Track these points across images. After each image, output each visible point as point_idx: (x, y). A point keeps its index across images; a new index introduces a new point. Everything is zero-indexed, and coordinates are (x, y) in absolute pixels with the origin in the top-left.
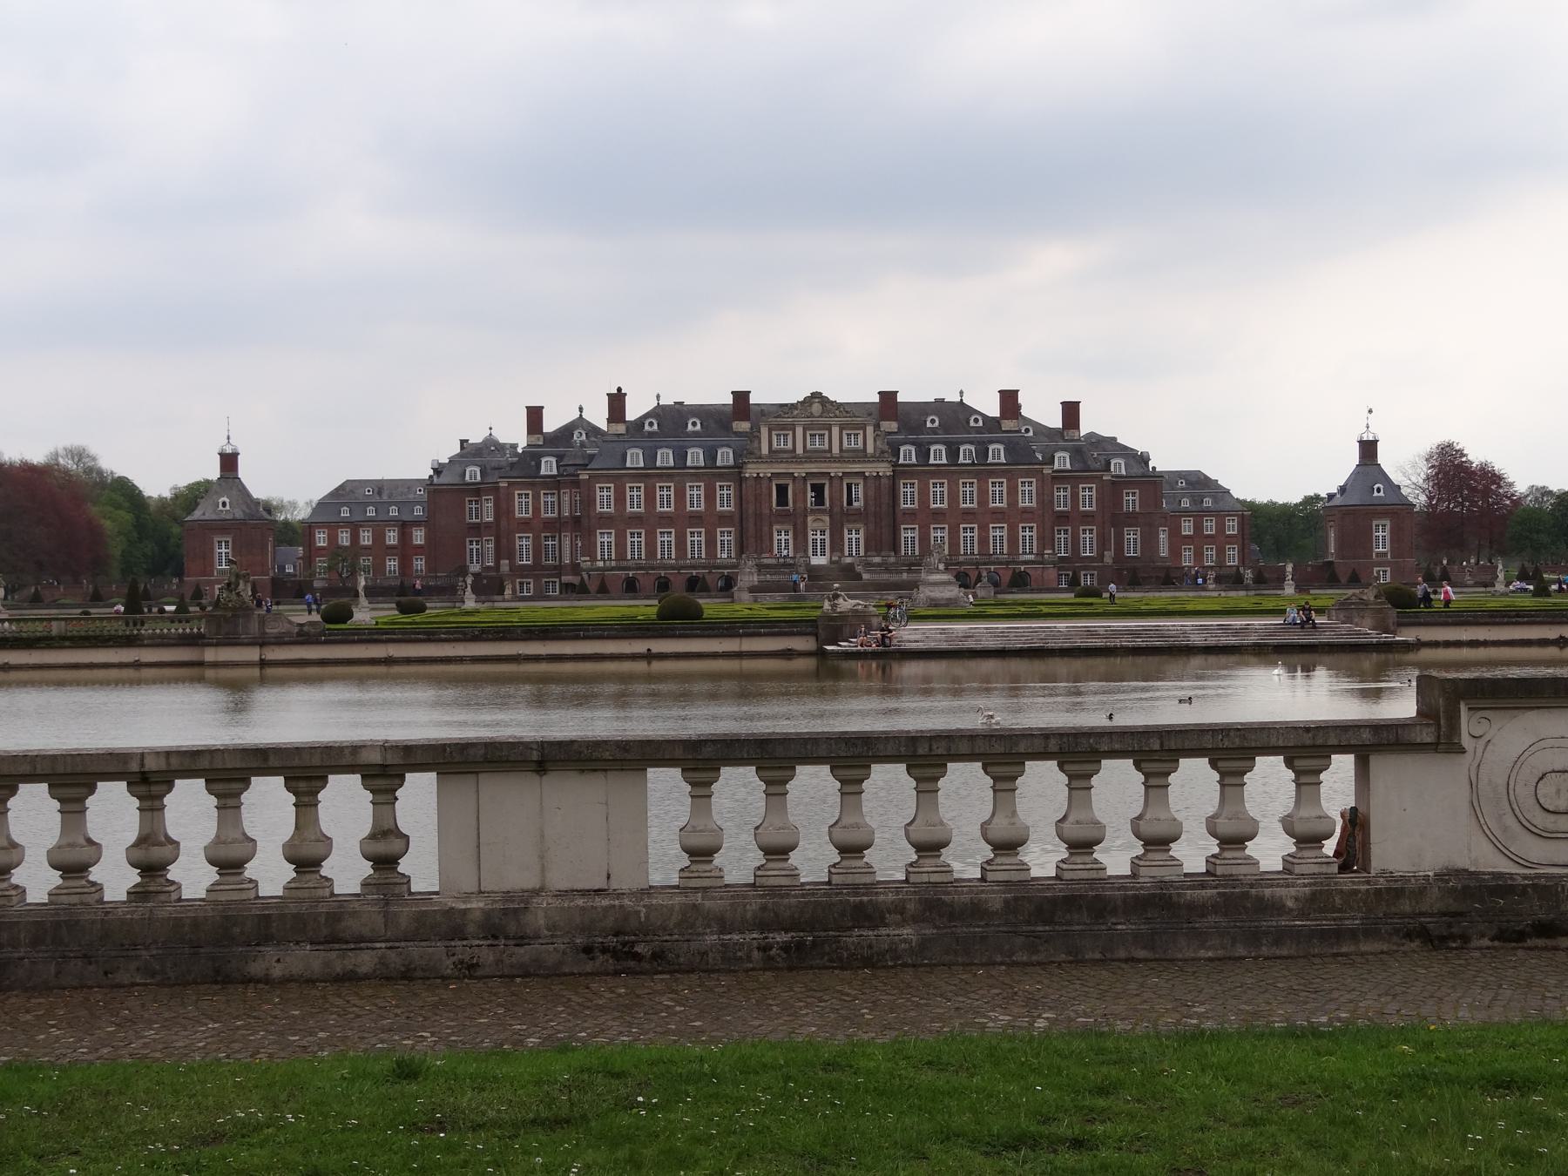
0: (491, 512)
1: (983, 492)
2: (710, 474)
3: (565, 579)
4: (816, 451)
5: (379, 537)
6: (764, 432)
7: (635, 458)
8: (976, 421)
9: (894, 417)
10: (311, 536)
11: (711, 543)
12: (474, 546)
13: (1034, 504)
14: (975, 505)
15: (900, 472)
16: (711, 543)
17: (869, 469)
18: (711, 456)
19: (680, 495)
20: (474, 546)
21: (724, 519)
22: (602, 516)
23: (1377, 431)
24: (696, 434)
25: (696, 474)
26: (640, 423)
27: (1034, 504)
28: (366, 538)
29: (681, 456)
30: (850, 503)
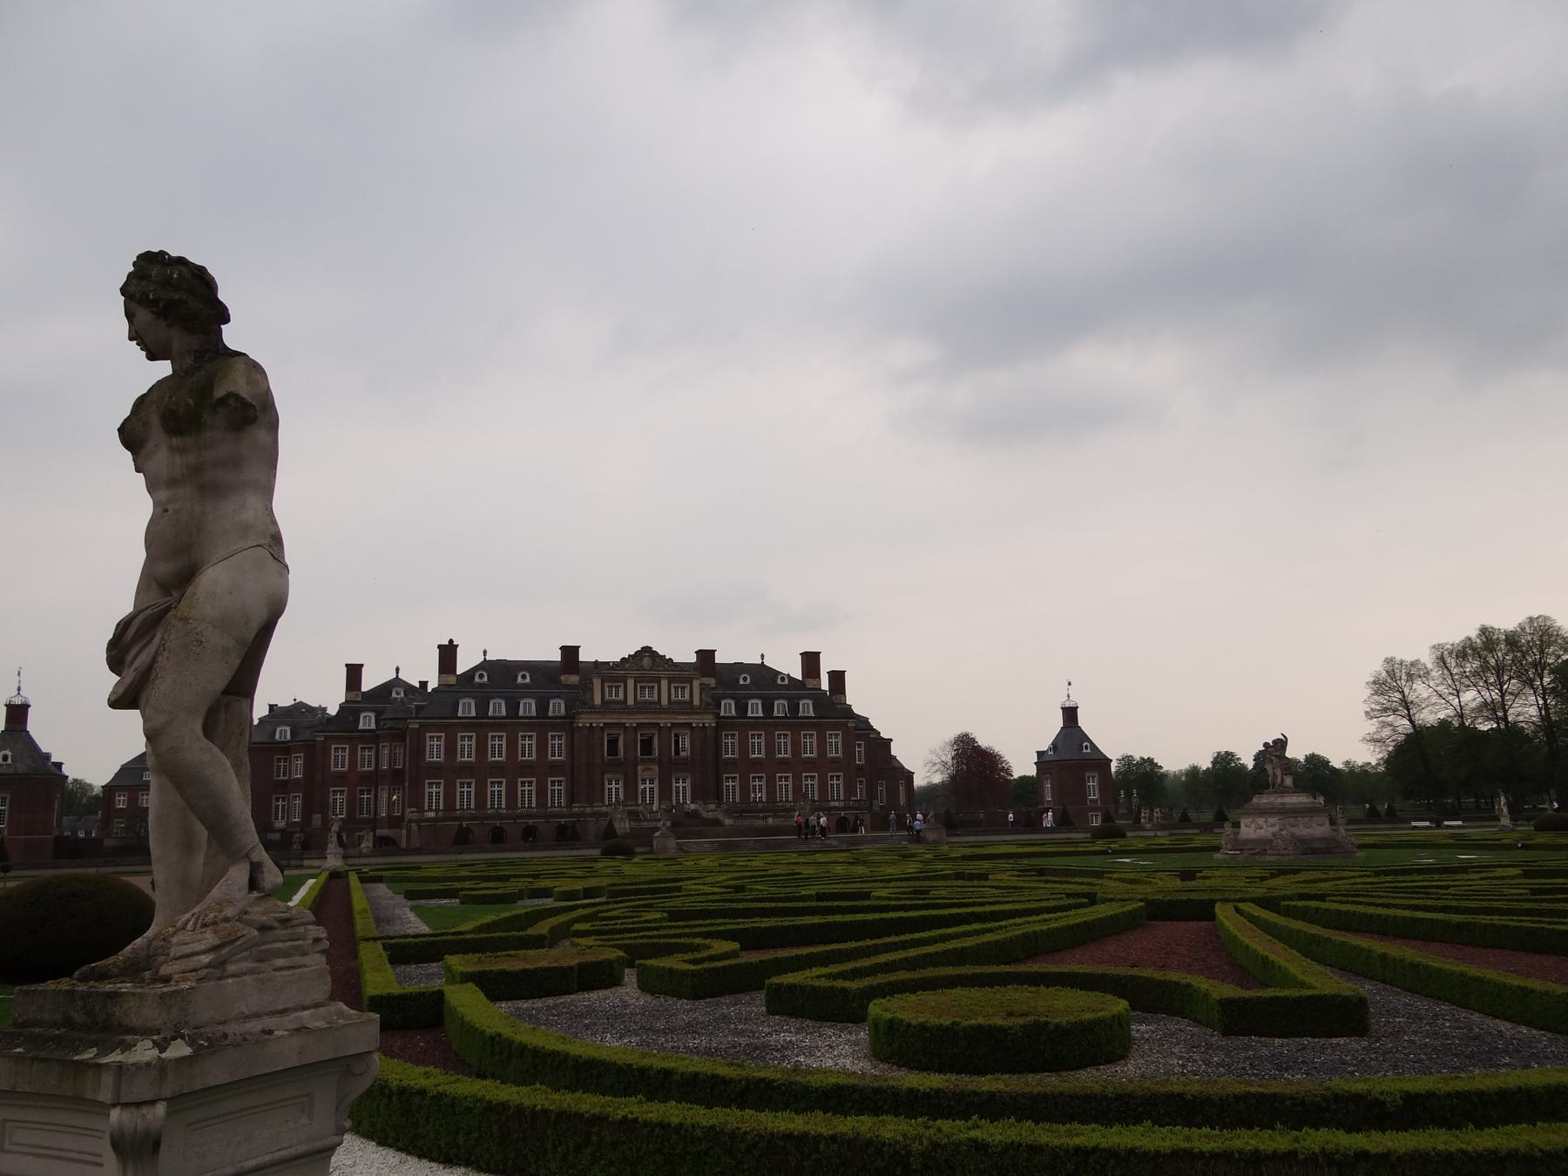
0: (300, 769)
2: (541, 724)
3: (380, 832)
6: (597, 683)
7: (467, 708)
9: (713, 675)
13: (840, 755)
14: (789, 755)
15: (723, 724)
16: (542, 792)
17: (695, 721)
18: (543, 708)
19: (512, 744)
21: (555, 768)
22: (432, 766)
23: (1076, 699)
24: (525, 686)
25: (529, 724)
26: (470, 674)
27: (840, 755)
29: (513, 708)
30: (677, 753)
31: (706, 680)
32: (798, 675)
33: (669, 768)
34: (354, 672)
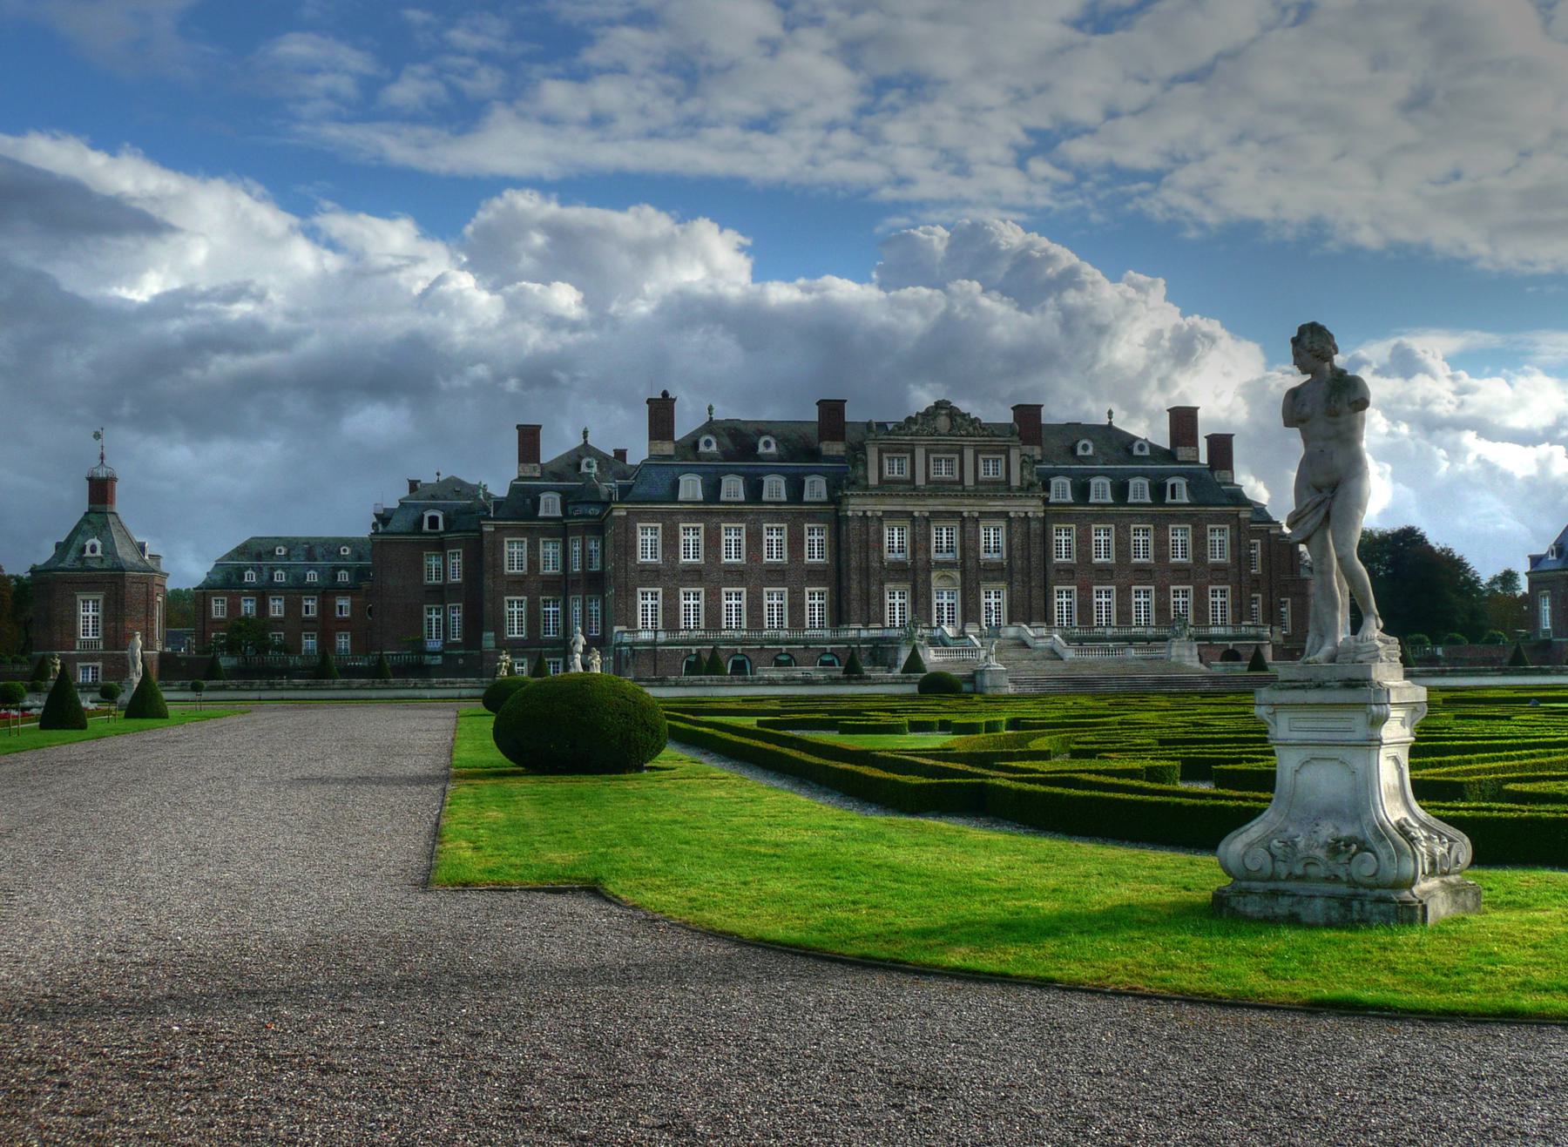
1: (1161, 543)
2: (795, 510)
4: (943, 482)
5: (293, 607)
8: (1141, 448)
10: (206, 607)
11: (796, 607)
12: (434, 616)
15: (1055, 514)
17: (1015, 508)
20: (434, 616)
21: (814, 575)
24: (770, 458)
26: (692, 444)
28: (276, 608)
29: (754, 491)
31: (1027, 449)
32: (1166, 444)
33: (972, 575)
34: (529, 438)
